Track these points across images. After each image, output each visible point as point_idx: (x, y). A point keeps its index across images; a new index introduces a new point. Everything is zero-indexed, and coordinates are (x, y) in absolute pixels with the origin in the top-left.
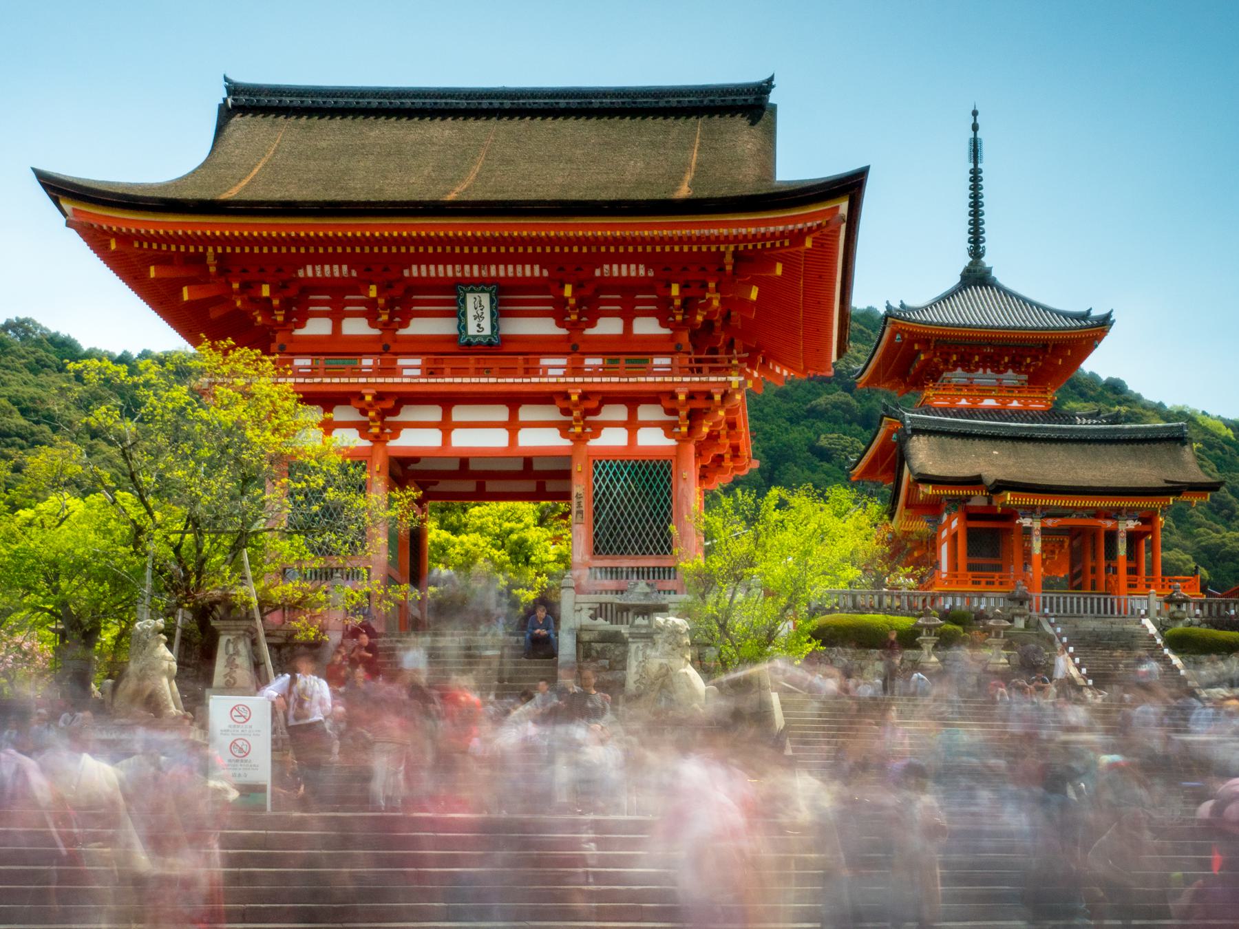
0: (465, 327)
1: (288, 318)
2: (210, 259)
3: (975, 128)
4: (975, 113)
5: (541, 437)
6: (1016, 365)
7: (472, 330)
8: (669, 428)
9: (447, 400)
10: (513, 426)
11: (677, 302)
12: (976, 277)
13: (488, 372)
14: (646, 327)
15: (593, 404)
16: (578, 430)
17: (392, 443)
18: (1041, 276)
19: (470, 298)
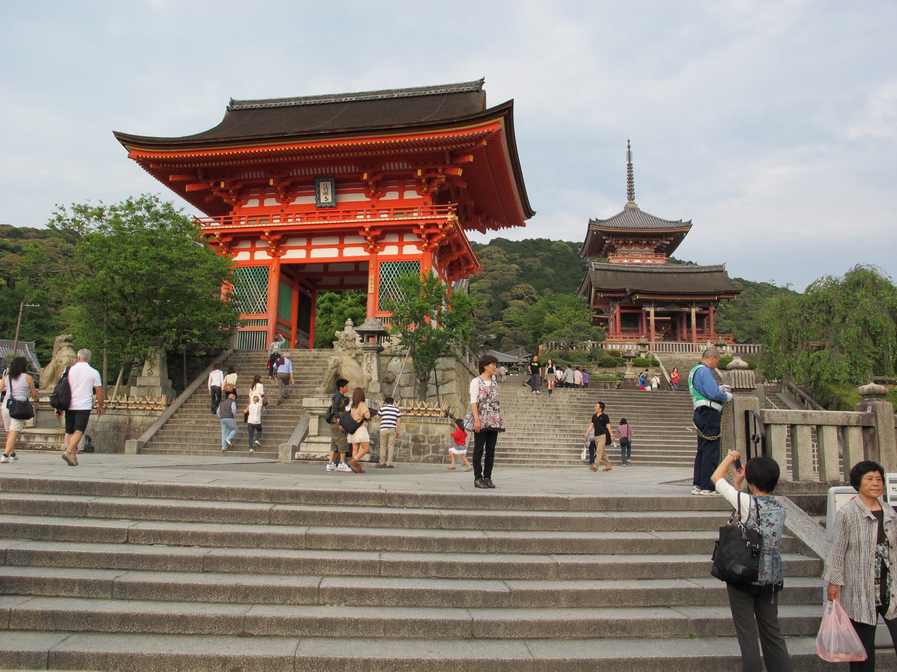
0: (319, 199)
1: (238, 200)
2: (199, 172)
3: (629, 147)
4: (629, 141)
5: (355, 252)
6: (648, 244)
7: (323, 200)
8: (419, 245)
9: (309, 235)
10: (341, 247)
11: (423, 181)
12: (631, 209)
13: (325, 218)
14: (411, 195)
15: (378, 233)
16: (371, 247)
17: (282, 257)
18: (660, 208)
19: (321, 184)
